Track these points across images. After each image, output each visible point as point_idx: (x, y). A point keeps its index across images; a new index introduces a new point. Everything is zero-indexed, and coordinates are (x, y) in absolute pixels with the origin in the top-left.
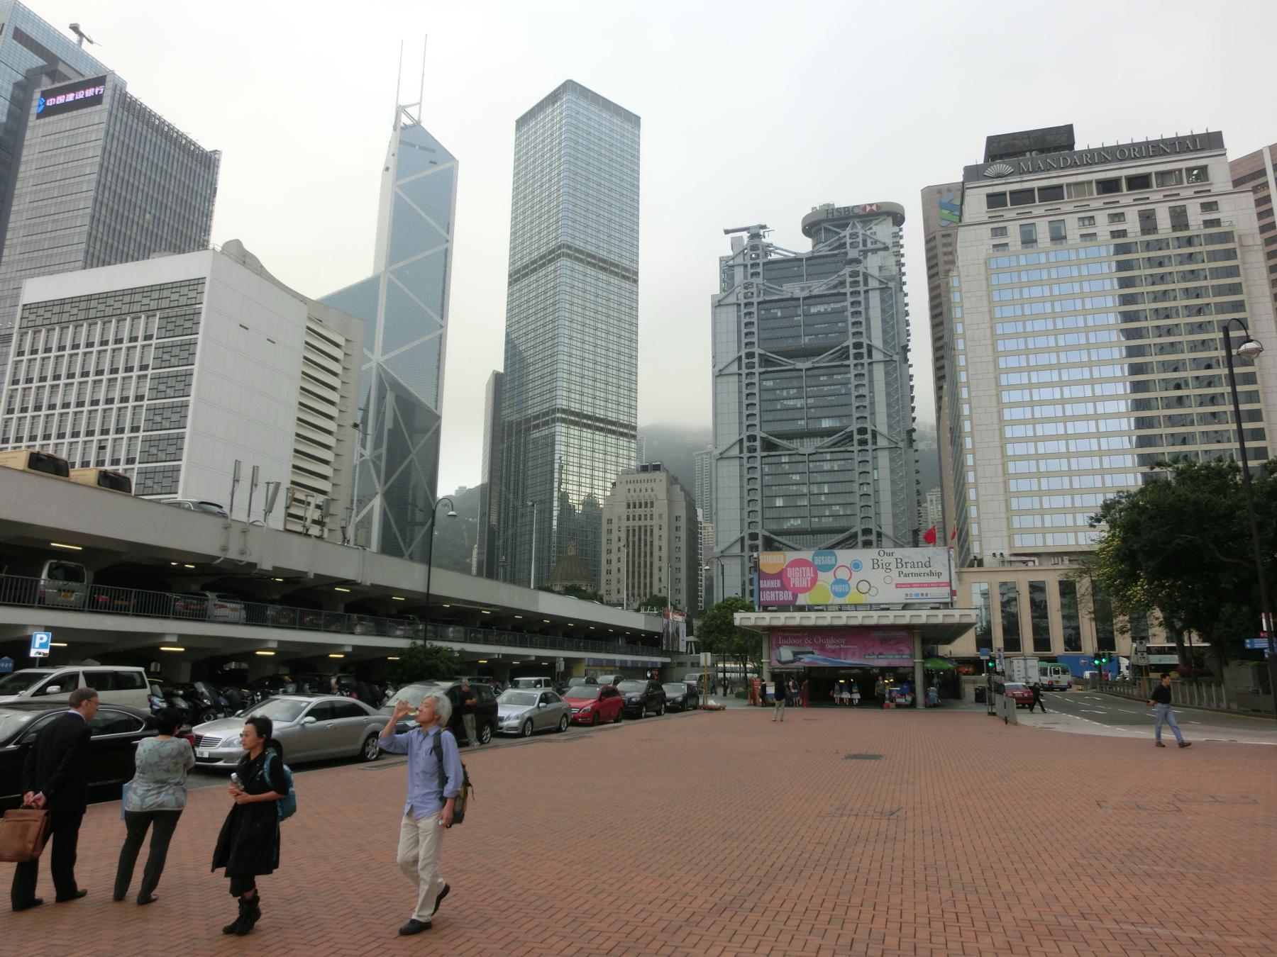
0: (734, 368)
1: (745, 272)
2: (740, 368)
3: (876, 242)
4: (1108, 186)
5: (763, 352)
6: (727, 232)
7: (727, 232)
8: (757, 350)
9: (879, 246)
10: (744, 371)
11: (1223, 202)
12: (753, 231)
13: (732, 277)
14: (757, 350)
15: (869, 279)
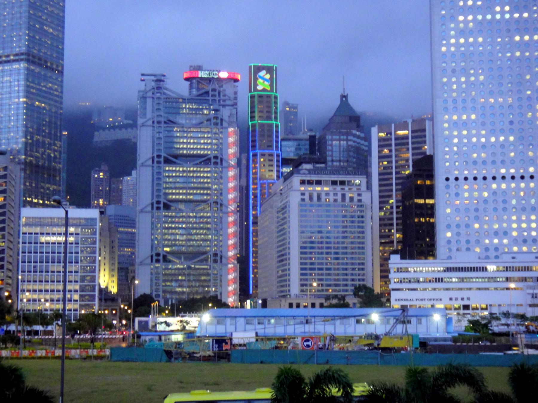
0: (150, 162)
1: (153, 102)
2: (153, 162)
3: (225, 95)
4: (334, 183)
5: (166, 156)
6: (143, 75)
7: (143, 75)
8: (163, 154)
9: (226, 98)
10: (155, 165)
11: (364, 194)
12: (159, 78)
13: (145, 103)
14: (163, 154)
15: (224, 122)
